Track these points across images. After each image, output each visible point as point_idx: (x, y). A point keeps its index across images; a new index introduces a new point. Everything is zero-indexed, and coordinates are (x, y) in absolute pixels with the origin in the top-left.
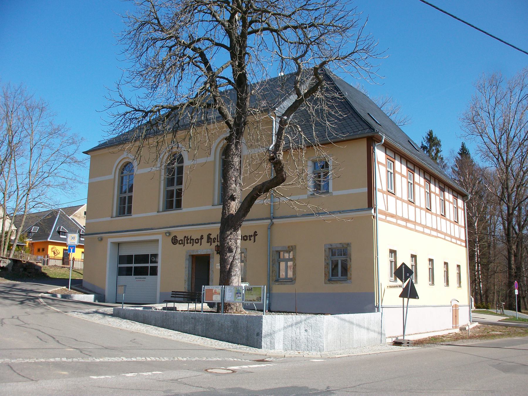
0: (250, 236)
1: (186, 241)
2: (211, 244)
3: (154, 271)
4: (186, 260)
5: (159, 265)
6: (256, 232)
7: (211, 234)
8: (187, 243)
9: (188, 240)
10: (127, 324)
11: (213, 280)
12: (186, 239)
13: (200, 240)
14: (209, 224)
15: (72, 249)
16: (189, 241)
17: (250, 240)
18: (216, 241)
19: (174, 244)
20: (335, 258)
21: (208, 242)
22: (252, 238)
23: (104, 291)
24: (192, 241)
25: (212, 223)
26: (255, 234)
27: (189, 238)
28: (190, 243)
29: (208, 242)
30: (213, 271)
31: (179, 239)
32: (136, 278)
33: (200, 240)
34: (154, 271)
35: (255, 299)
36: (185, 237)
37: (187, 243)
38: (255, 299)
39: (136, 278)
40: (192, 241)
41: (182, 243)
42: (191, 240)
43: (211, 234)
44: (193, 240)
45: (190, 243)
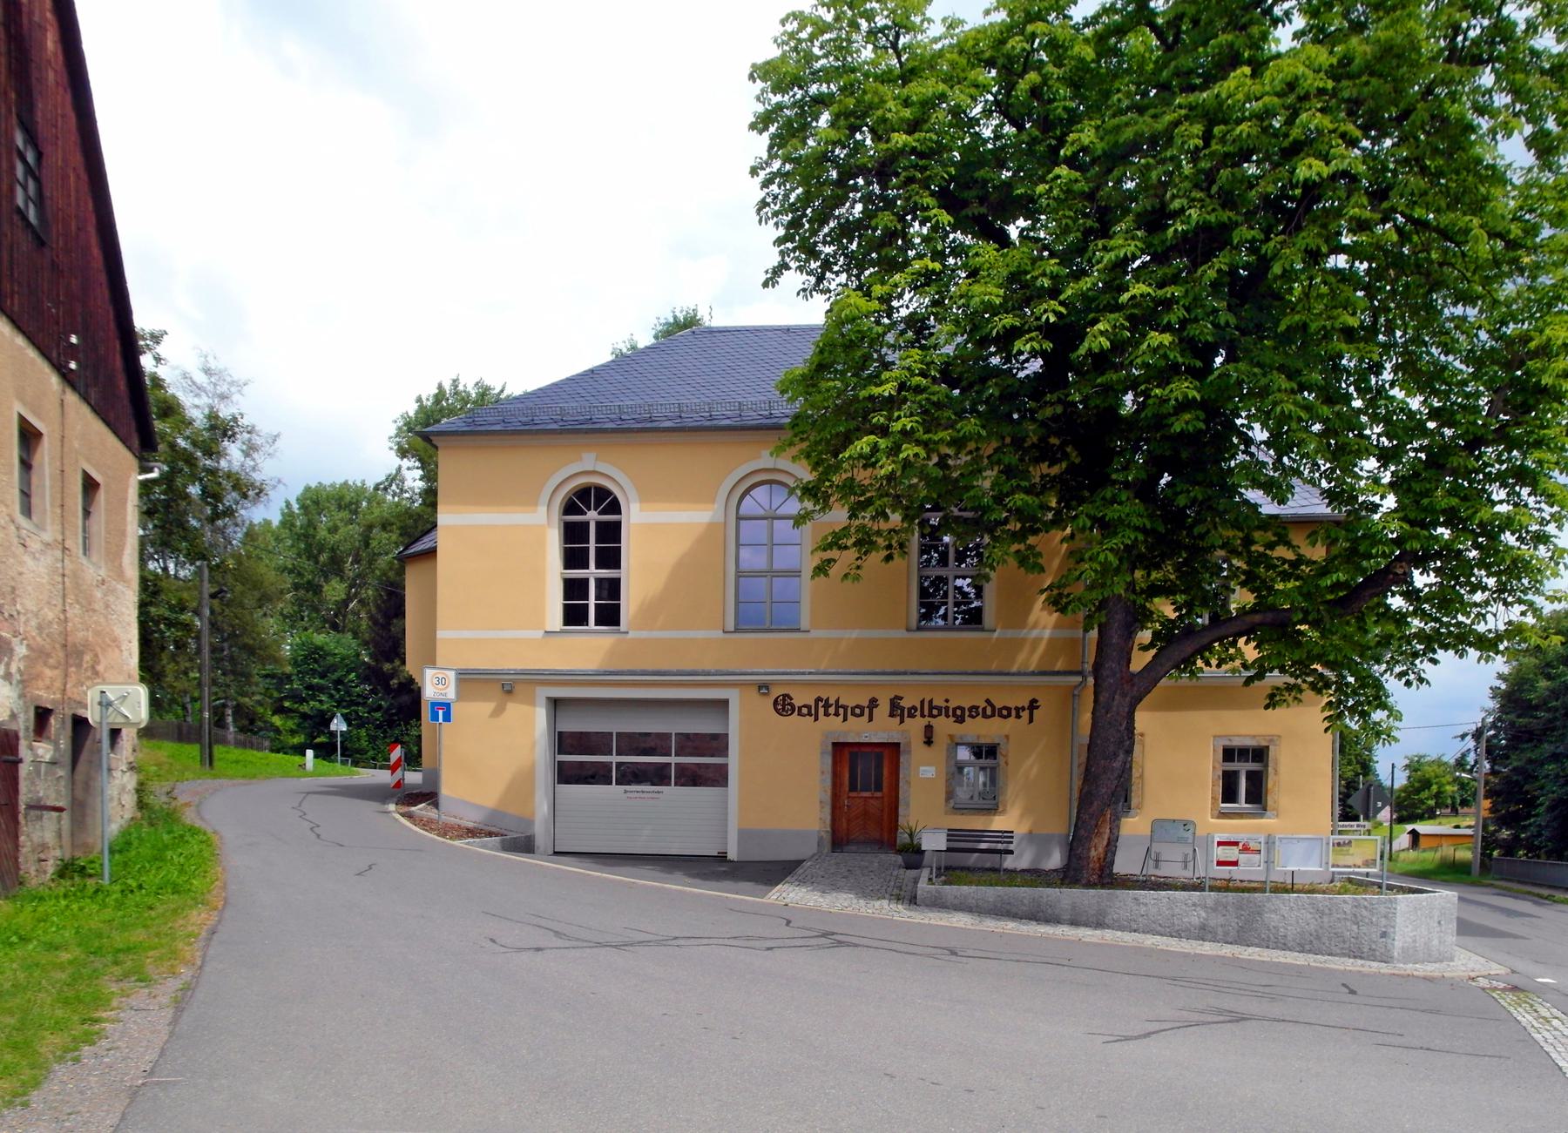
0: (1017, 709)
1: (821, 711)
2: (902, 721)
3: (718, 777)
4: (823, 753)
5: (734, 761)
6: (1034, 701)
7: (901, 698)
8: (827, 715)
9: (827, 706)
10: (1177, 928)
11: (908, 805)
12: (821, 704)
13: (867, 711)
14: (905, 673)
15: (441, 712)
16: (832, 710)
17: (1018, 716)
18: (918, 713)
19: (777, 710)
20: (1231, 766)
21: (892, 715)
22: (1025, 714)
23: (530, 822)
24: (841, 711)
25: (912, 674)
26: (1033, 706)
27: (832, 701)
28: (837, 714)
29: (892, 715)
30: (908, 783)
31: (797, 703)
32: (626, 792)
33: (867, 711)
34: (718, 777)
35: (1359, 862)
36: (818, 700)
37: (827, 715)
38: (1359, 862)
39: (626, 792)
40: (841, 711)
41: (811, 712)
42: (838, 707)
43: (901, 698)
44: (845, 708)
45: (837, 714)
